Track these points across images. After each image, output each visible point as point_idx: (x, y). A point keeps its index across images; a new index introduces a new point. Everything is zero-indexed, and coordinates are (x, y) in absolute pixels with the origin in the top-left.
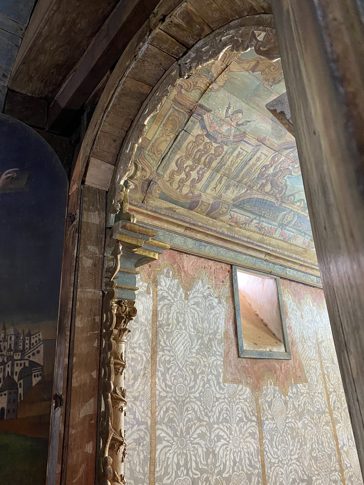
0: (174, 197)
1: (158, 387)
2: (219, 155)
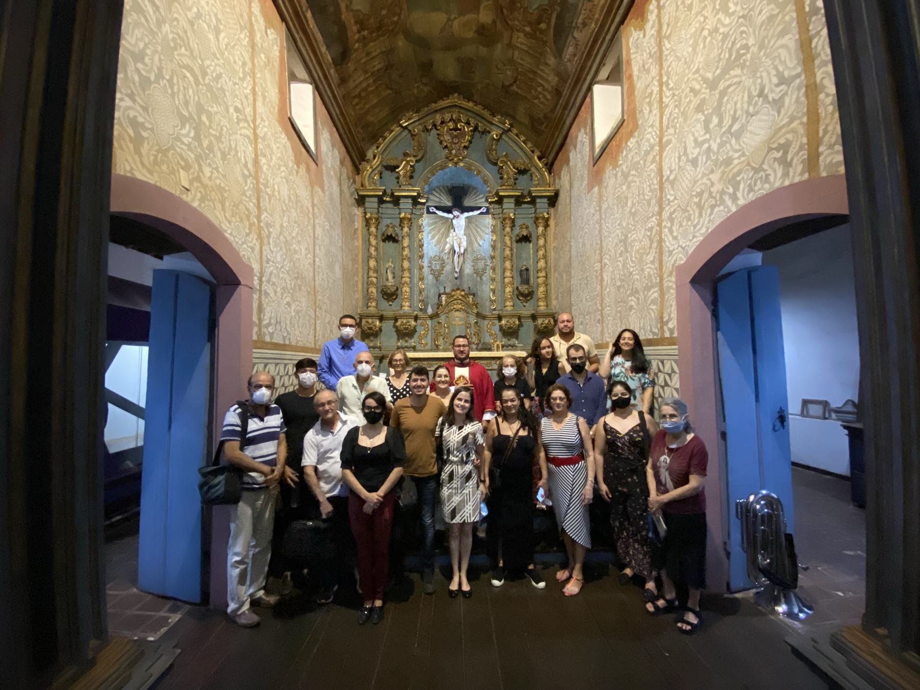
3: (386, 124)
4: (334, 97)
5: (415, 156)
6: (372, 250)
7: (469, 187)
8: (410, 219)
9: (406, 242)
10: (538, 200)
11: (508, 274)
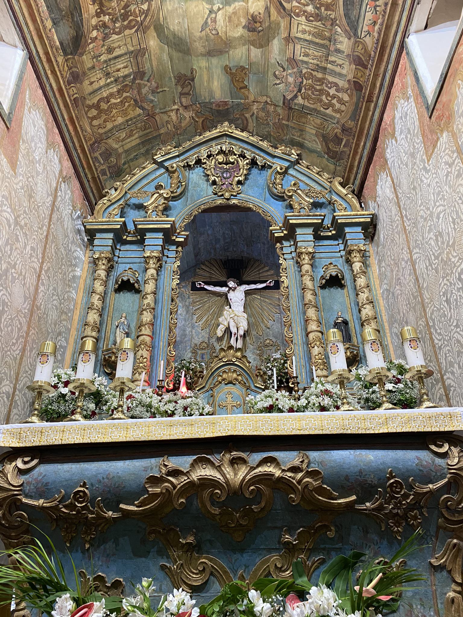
0: (353, 107)
1: (407, 228)
2: (311, 73)
3: (136, 158)
4: (60, 90)
5: (172, 192)
6: (96, 300)
7: (249, 260)
8: (159, 259)
9: (150, 287)
10: (347, 230)
11: (313, 326)
